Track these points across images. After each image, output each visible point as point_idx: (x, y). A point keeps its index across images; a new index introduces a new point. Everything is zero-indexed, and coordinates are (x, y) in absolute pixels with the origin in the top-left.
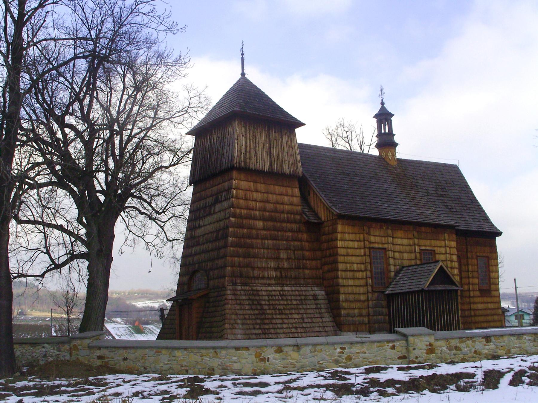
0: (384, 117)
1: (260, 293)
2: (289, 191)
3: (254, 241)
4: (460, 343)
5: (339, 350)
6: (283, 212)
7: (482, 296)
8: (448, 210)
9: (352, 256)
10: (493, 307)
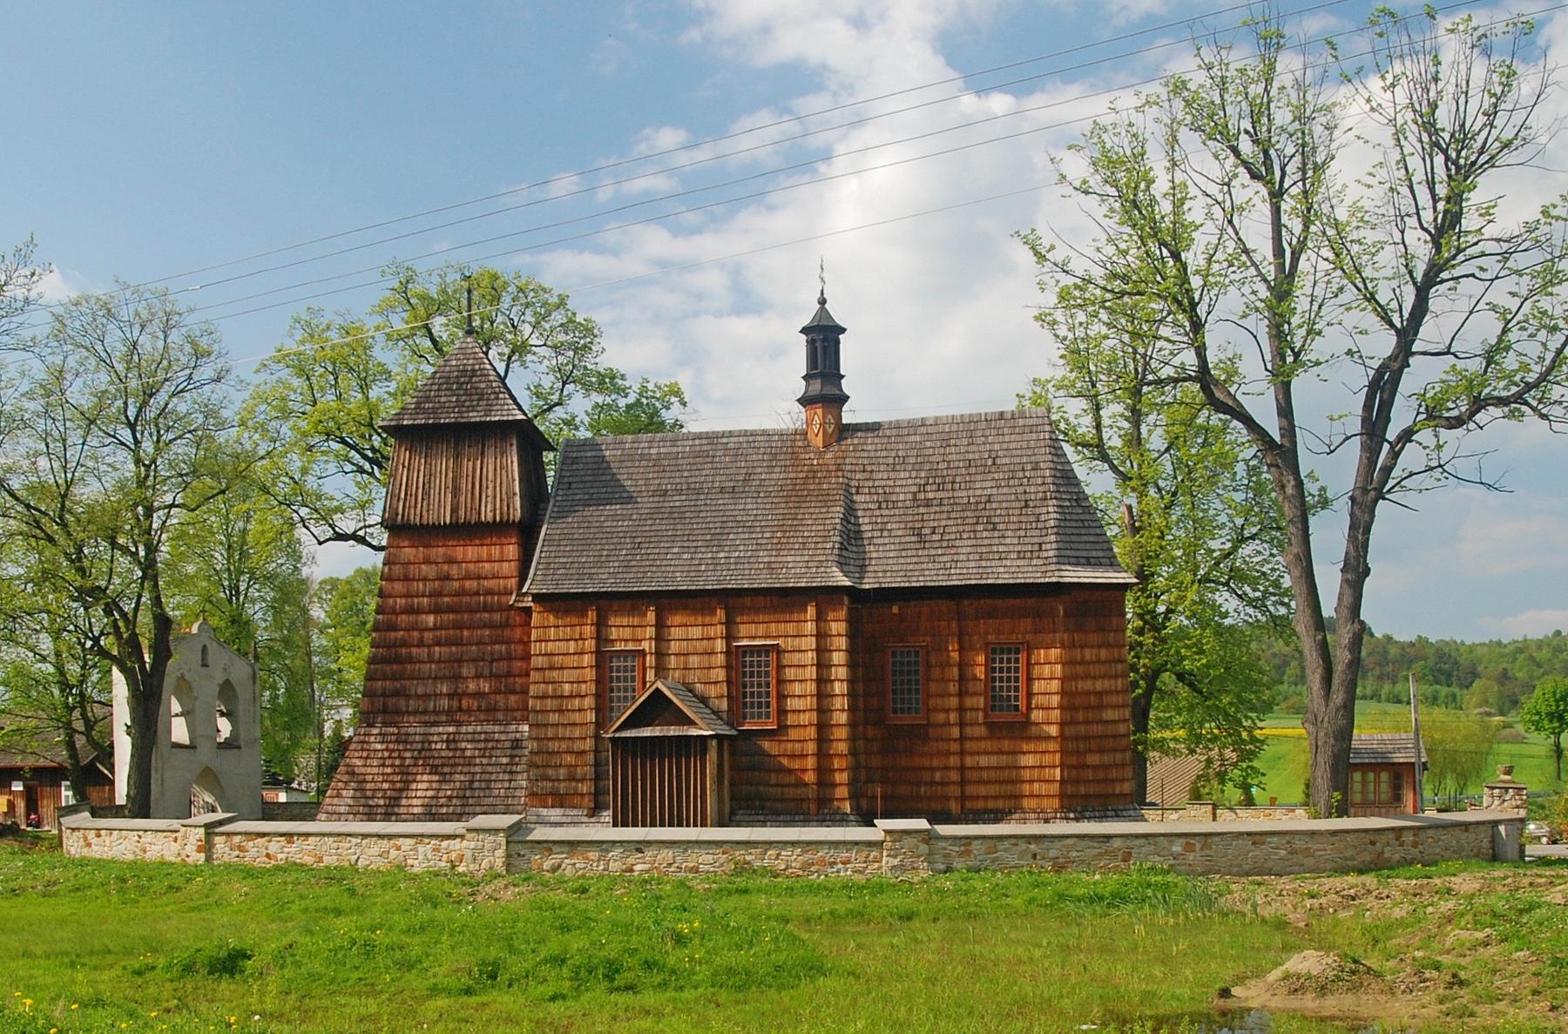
0: (824, 339)
1: (411, 739)
3: (414, 650)
6: (477, 594)
7: (991, 737)
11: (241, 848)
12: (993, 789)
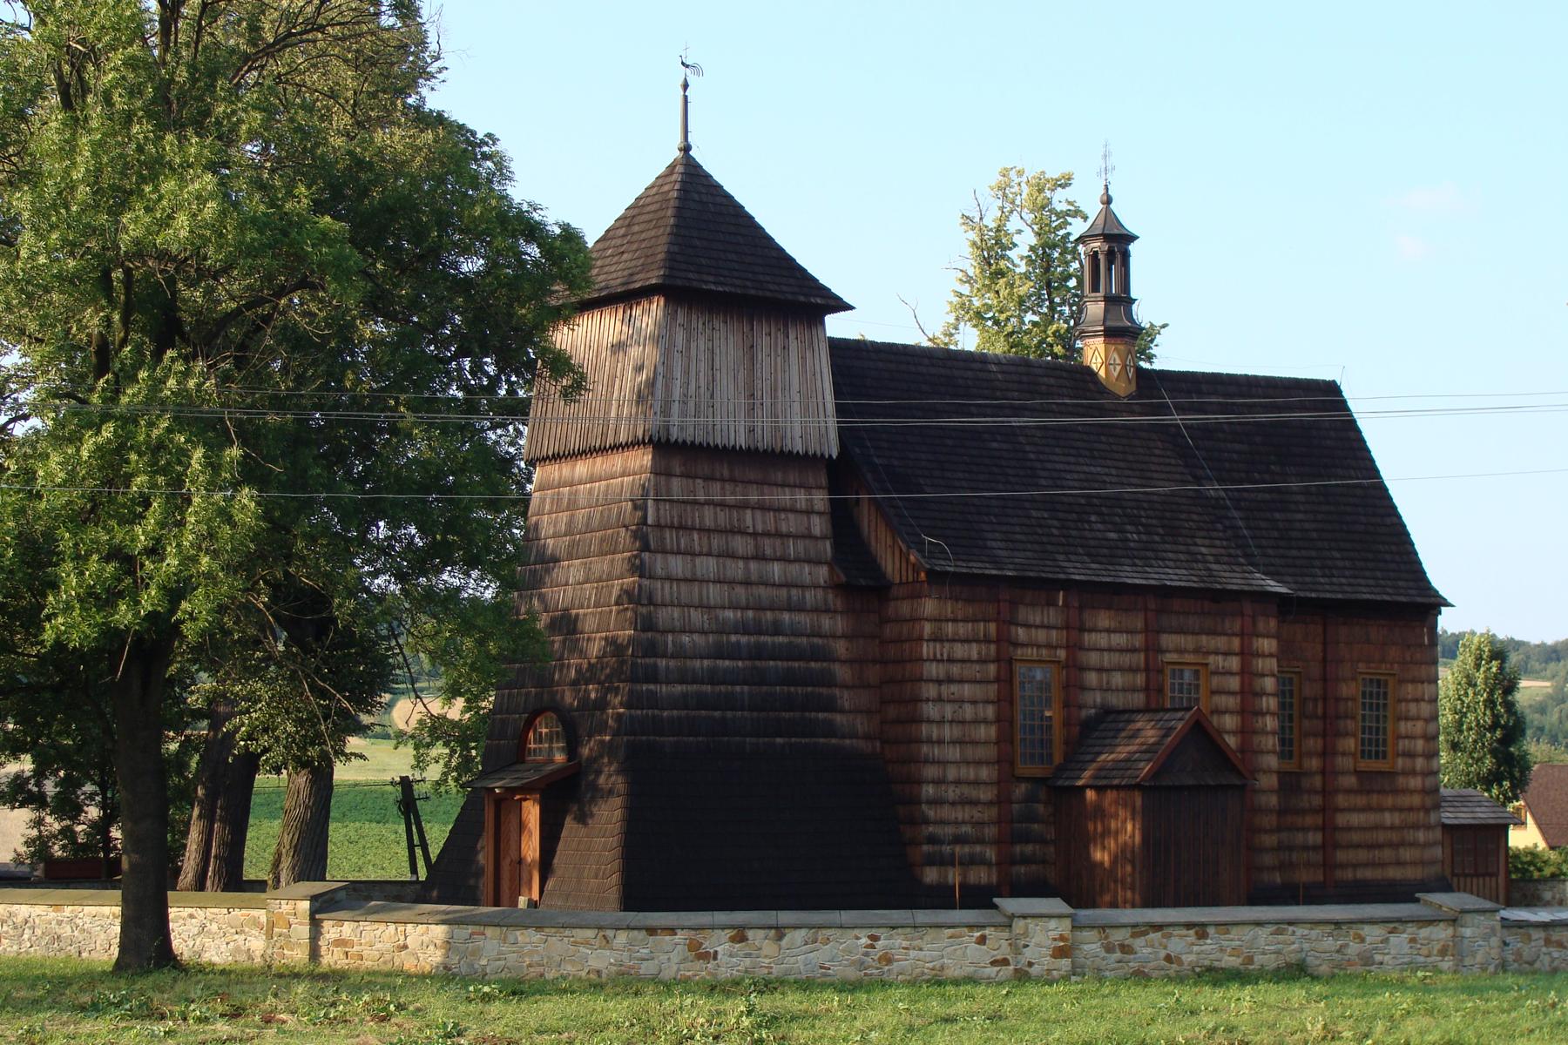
2: (801, 497)
4: (1134, 935)
5: (864, 941)
8: (1276, 534)
9: (961, 681)
10: (1397, 822)
11: (1126, 949)
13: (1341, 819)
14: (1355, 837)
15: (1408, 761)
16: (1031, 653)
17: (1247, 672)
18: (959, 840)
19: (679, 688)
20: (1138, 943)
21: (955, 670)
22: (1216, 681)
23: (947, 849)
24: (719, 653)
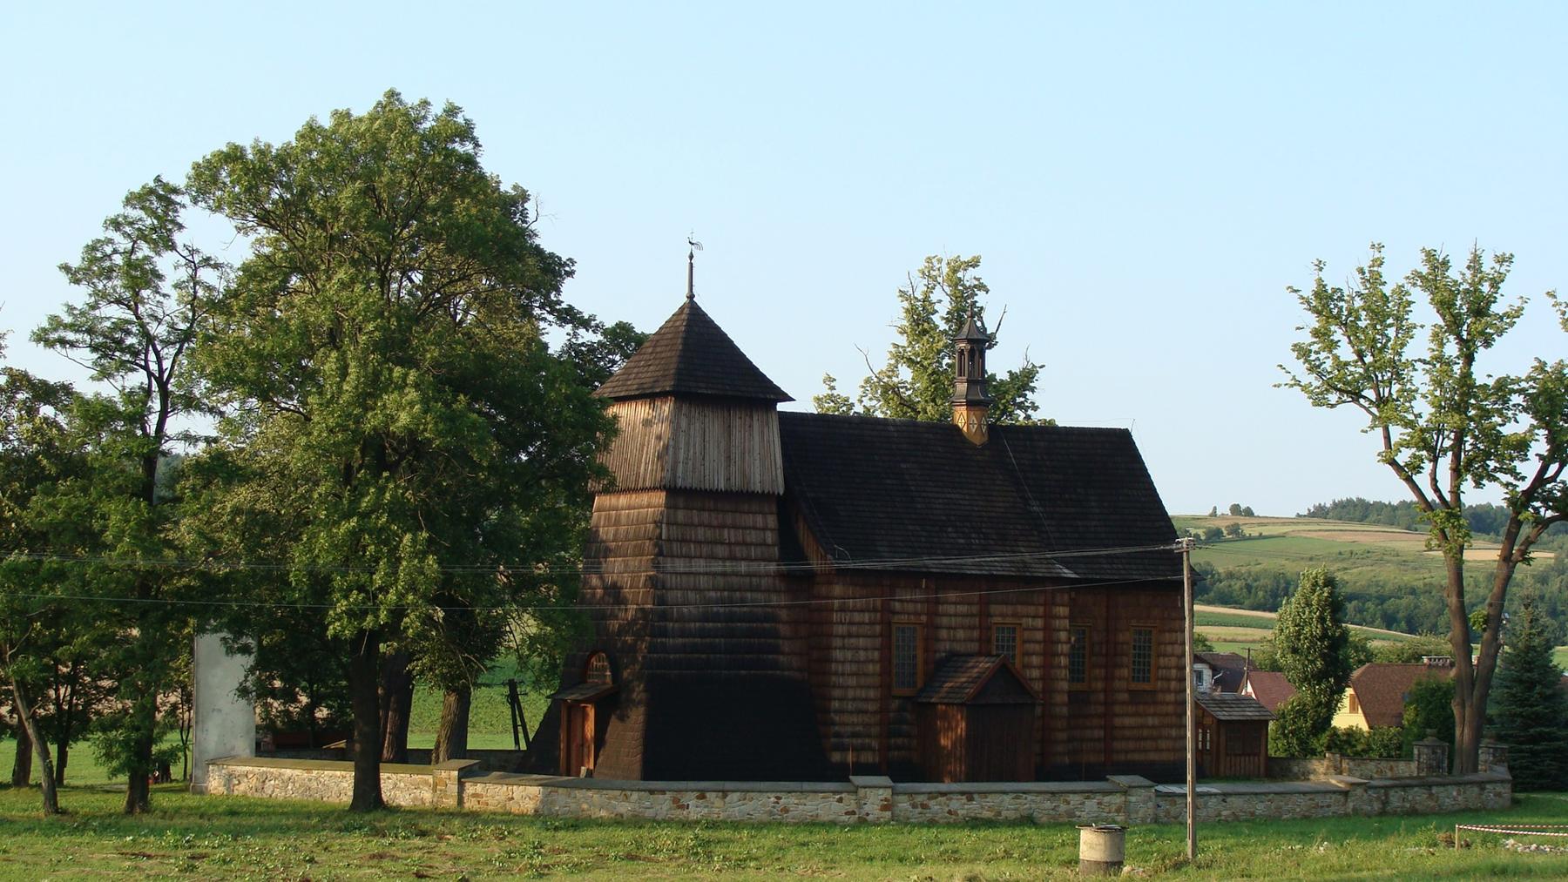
2: (759, 519)
9: (858, 636)
11: (924, 806)
12: (1131, 745)
13: (1118, 721)
14: (1127, 733)
15: (1165, 684)
16: (904, 618)
17: (1048, 629)
18: (855, 735)
19: (680, 640)
20: (932, 803)
21: (854, 629)
22: (1027, 634)
23: (846, 740)
24: (705, 618)
